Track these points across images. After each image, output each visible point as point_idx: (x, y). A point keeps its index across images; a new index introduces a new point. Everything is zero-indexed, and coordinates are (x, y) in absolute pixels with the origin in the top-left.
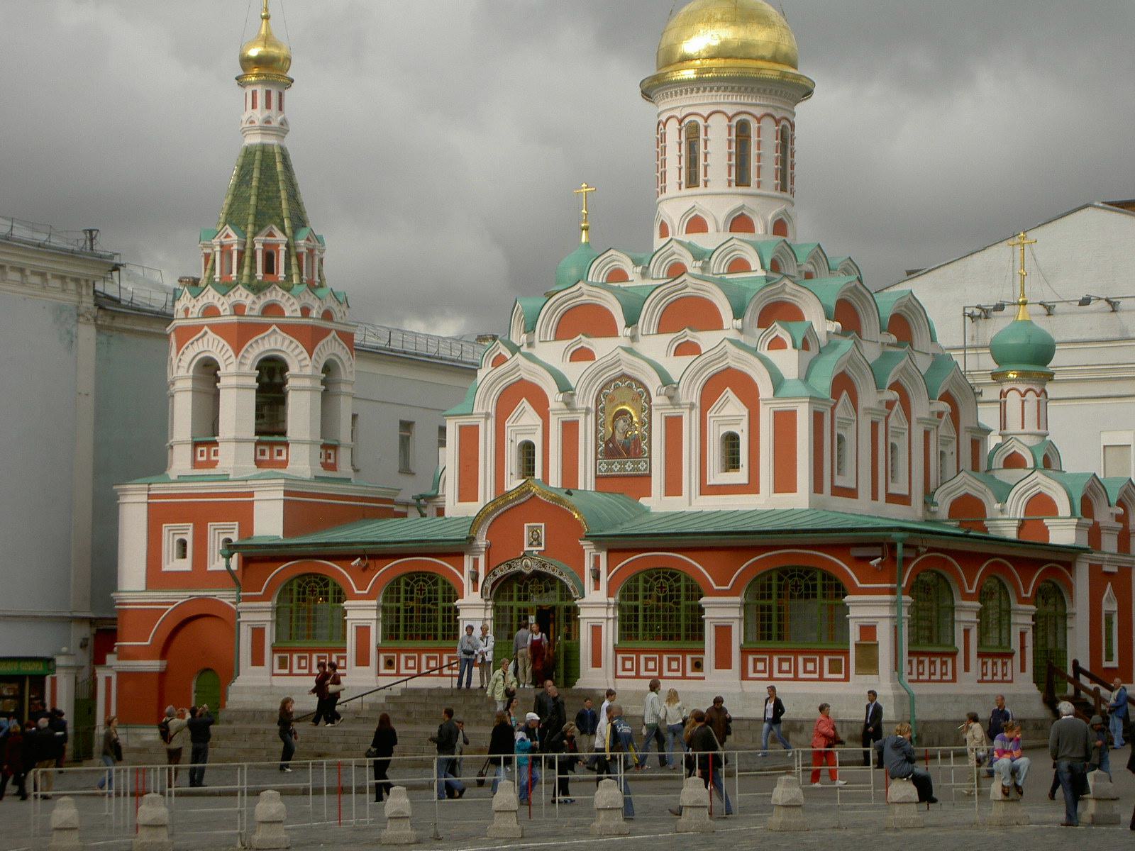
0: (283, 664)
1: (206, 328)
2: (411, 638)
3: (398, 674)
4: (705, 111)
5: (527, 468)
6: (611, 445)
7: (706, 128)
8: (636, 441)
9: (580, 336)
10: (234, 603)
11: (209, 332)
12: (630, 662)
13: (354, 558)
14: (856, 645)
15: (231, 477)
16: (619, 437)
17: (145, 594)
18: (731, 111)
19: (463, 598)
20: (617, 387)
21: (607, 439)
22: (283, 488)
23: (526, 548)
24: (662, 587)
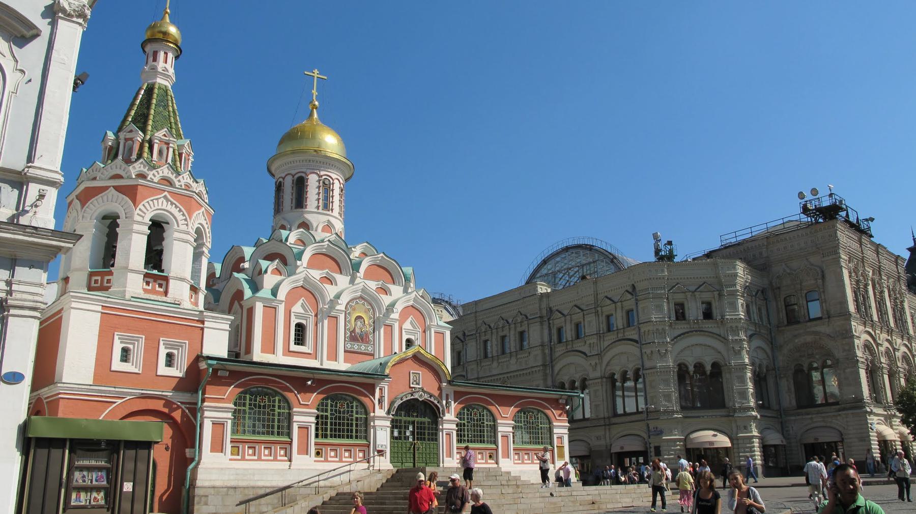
0: (236, 450)
1: (166, 193)
2: (335, 437)
3: (326, 461)
4: (334, 176)
5: (300, 339)
6: (353, 334)
7: (333, 184)
8: (367, 335)
9: (327, 270)
10: (182, 403)
11: (169, 197)
12: (346, 456)
13: (309, 379)
14: (557, 446)
15: (181, 306)
16: (358, 330)
17: (92, 387)
18: (341, 181)
19: (374, 412)
20: (357, 303)
21: (351, 330)
22: (230, 323)
23: (412, 386)
24: (475, 414)
